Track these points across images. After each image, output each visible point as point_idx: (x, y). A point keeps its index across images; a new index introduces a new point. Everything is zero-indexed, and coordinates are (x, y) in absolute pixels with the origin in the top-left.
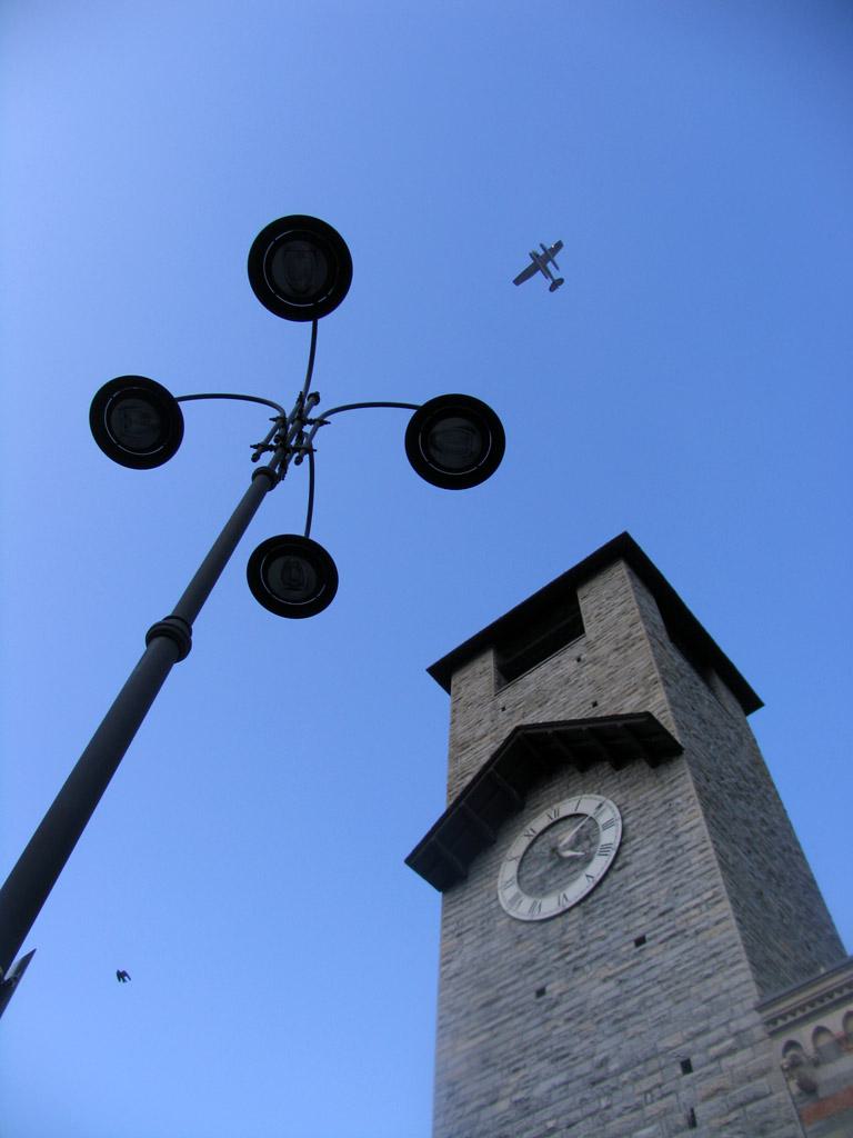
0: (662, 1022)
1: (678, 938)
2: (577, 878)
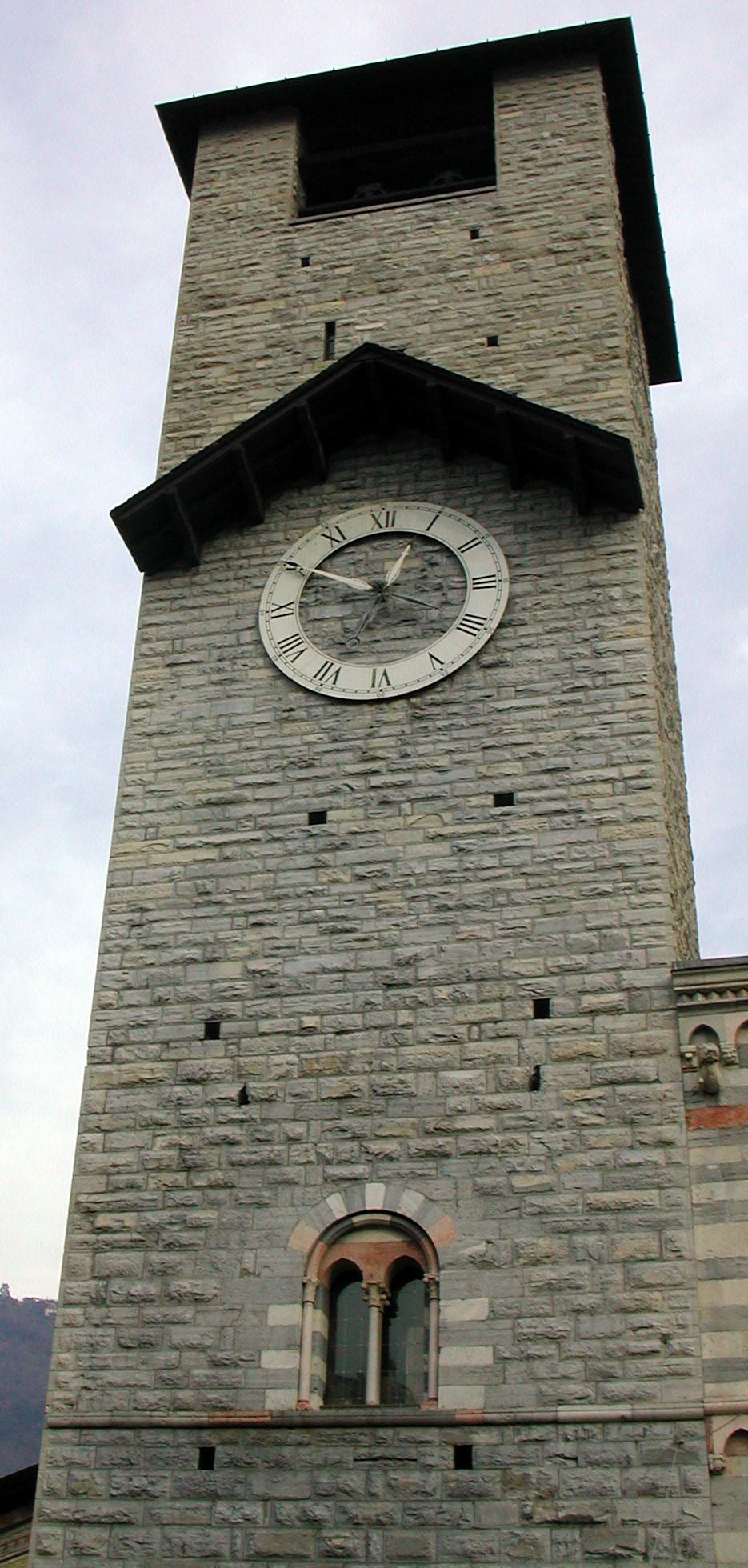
0: (516, 934)
1: (570, 818)
2: (415, 651)
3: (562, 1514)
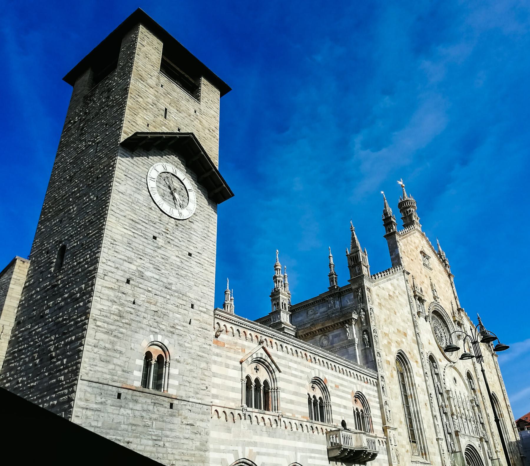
1: (201, 265)
3: (188, 423)
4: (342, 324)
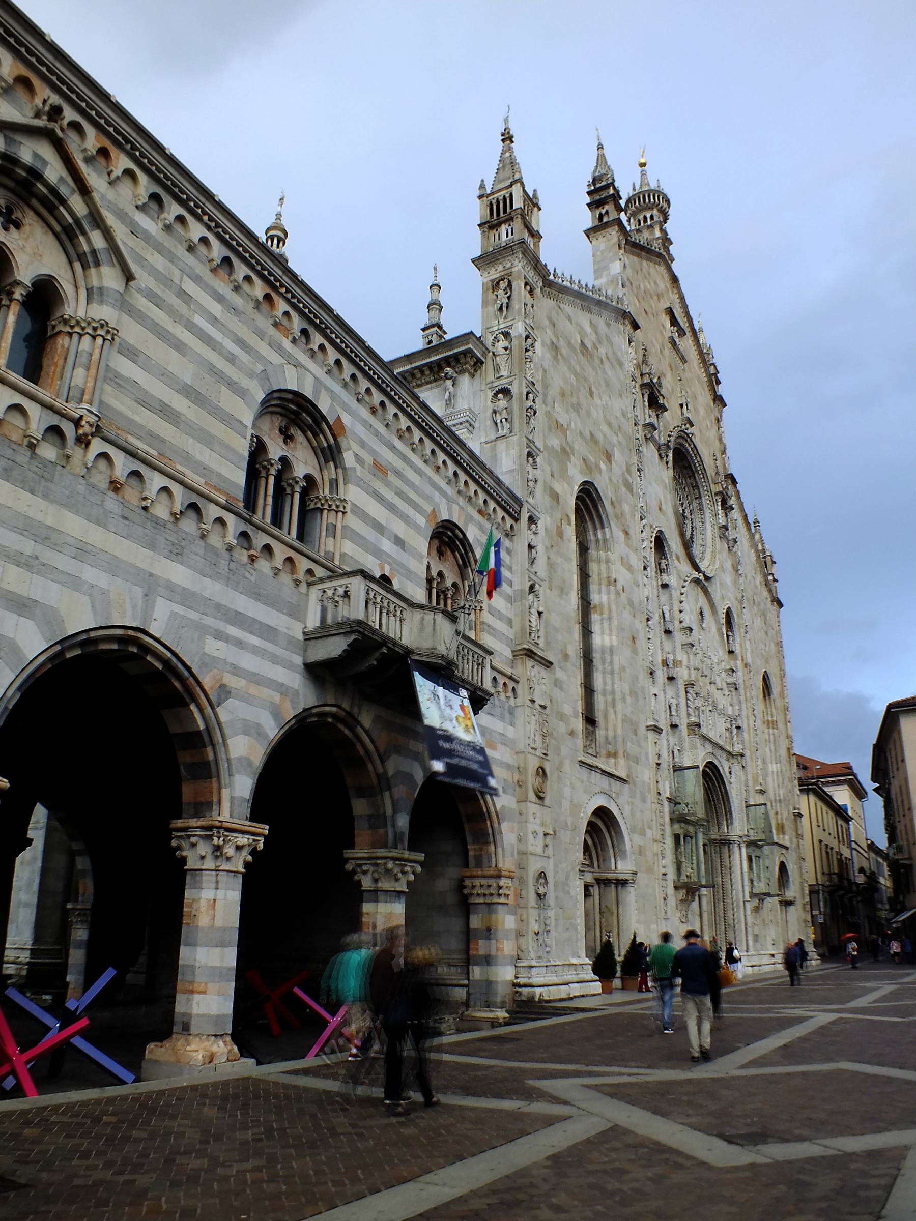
4: (436, 369)
